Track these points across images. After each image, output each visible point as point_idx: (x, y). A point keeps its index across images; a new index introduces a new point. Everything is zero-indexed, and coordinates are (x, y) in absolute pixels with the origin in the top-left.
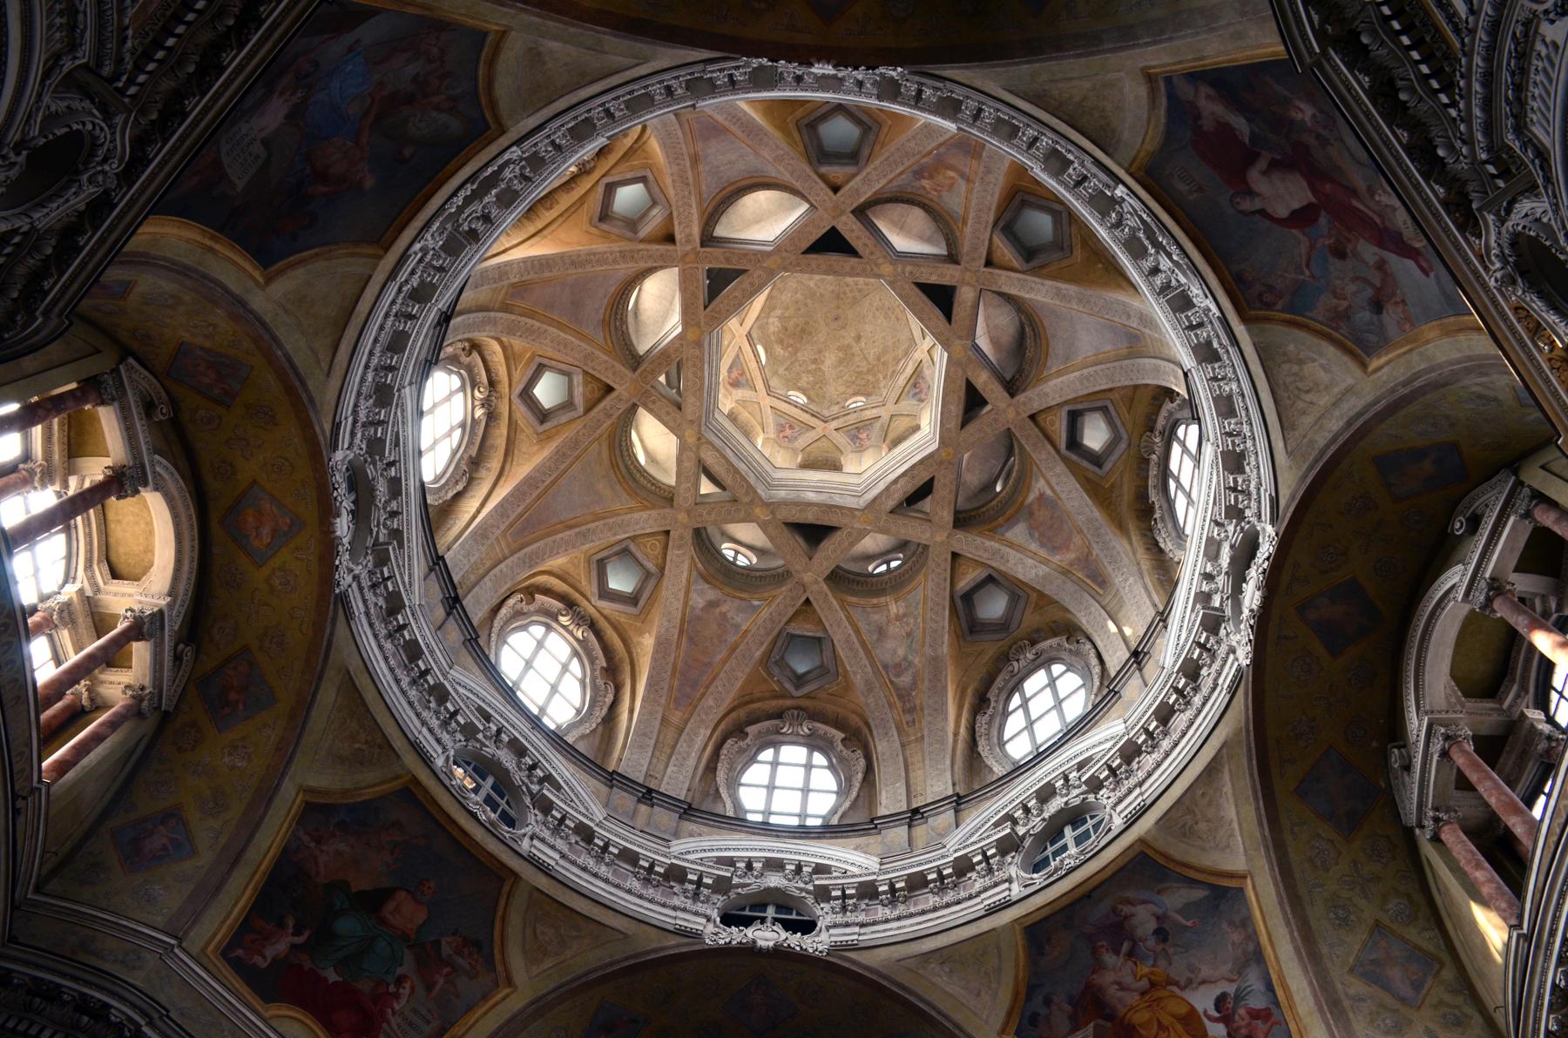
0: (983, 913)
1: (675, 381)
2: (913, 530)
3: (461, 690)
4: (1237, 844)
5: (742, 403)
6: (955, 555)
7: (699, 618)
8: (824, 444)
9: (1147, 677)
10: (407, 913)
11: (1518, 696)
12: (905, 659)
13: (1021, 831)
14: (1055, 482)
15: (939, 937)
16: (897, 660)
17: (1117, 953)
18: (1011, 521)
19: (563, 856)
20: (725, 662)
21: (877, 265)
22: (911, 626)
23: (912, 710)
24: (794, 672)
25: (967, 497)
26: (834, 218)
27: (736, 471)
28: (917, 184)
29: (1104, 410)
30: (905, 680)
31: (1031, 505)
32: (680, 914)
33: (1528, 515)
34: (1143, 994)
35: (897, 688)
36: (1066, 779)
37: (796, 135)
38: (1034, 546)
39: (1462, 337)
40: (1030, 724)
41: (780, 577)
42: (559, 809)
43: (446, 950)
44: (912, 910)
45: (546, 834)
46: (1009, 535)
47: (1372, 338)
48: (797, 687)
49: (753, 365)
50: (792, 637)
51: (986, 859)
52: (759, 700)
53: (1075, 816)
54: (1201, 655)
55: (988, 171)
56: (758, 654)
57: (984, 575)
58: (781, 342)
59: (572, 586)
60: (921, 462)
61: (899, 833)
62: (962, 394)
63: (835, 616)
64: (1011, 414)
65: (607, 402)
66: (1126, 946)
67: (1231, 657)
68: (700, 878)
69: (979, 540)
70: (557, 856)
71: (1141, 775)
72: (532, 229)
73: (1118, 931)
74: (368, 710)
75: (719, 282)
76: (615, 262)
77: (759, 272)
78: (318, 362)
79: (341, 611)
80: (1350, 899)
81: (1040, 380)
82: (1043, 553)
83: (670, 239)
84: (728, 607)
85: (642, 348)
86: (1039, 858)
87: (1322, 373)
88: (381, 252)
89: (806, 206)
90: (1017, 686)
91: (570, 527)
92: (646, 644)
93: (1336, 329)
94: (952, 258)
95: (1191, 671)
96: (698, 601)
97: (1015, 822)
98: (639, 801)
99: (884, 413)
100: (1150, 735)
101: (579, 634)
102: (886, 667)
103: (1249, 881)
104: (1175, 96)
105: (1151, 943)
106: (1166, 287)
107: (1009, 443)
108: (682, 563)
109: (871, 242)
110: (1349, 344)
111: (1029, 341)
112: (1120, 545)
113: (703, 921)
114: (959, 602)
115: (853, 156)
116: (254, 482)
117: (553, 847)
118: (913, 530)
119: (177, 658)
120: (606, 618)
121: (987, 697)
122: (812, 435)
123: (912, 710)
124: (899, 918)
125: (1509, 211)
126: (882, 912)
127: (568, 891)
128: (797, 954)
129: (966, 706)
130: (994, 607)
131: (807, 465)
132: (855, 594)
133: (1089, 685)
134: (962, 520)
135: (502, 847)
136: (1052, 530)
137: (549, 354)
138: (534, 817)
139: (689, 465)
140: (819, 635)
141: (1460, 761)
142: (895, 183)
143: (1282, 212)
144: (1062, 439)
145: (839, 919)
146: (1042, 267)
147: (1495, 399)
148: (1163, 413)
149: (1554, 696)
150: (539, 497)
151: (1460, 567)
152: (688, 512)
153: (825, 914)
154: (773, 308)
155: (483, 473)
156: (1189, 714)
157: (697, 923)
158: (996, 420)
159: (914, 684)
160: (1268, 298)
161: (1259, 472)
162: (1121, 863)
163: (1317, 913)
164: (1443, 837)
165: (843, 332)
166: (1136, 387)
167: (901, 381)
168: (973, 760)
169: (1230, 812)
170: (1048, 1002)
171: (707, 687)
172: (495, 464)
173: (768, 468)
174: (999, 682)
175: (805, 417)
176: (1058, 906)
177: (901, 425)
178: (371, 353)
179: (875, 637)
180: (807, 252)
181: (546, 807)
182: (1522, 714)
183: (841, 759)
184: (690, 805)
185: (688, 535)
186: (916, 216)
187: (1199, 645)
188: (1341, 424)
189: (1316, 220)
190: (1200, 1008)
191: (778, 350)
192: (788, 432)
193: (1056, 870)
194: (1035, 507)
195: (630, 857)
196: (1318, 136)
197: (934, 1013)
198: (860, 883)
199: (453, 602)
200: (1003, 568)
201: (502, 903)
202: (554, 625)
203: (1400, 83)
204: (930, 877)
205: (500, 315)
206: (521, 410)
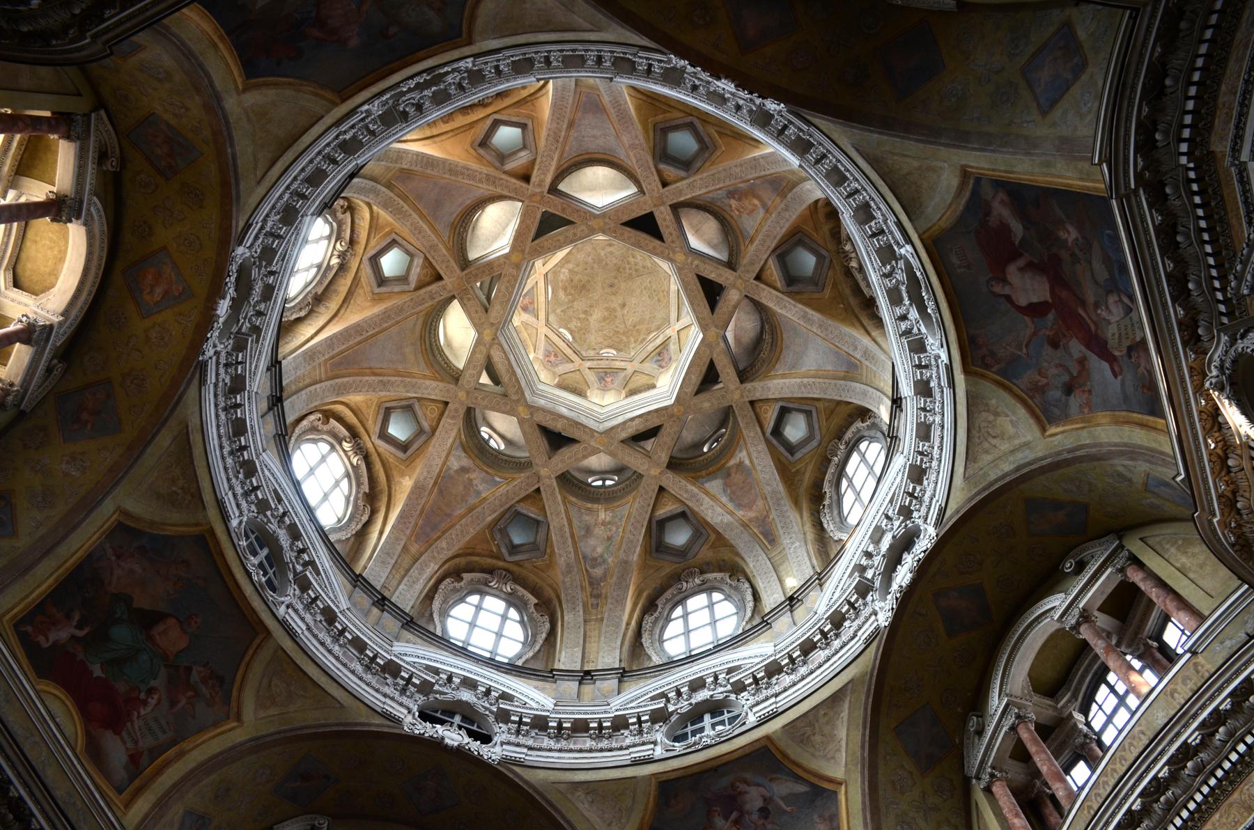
0: (628, 762)
1: (490, 288)
2: (634, 460)
3: (267, 472)
4: (841, 759)
5: (525, 325)
6: (661, 489)
7: (451, 477)
8: (577, 376)
9: (796, 618)
10: (171, 637)
11: (1069, 701)
12: (601, 556)
13: (671, 708)
14: (754, 456)
17: (726, 818)
18: (711, 476)
19: (309, 629)
20: (462, 517)
22: (613, 532)
23: (598, 596)
24: (511, 541)
25: (688, 446)
27: (514, 373)
28: (726, 201)
29: (808, 414)
30: (598, 572)
31: (729, 468)
32: (388, 701)
33: (1122, 570)
35: (590, 577)
36: (716, 678)
38: (724, 499)
39: (1126, 428)
40: (687, 632)
41: (522, 466)
42: (315, 591)
44: (572, 746)
45: (300, 607)
46: (707, 485)
47: (1057, 412)
48: (510, 554)
49: (542, 299)
50: (518, 514)
51: (640, 722)
52: (478, 555)
53: (715, 708)
54: (848, 611)
55: (787, 209)
56: (490, 519)
57: (680, 510)
58: (565, 289)
59: (361, 422)
60: (657, 411)
61: (572, 686)
62: (704, 369)
63: (556, 506)
64: (736, 396)
65: (434, 287)
66: (734, 815)
67: (873, 617)
68: (411, 677)
69: (684, 482)
70: (304, 628)
71: (777, 689)
72: (428, 133)
73: (732, 803)
74: (192, 463)
75: (550, 224)
76: (480, 181)
77: (583, 227)
78: (255, 169)
79: (197, 375)
81: (766, 376)
82: (730, 506)
83: (526, 178)
84: (476, 476)
85: (473, 255)
86: (680, 732)
87: (1010, 427)
88: (338, 100)
89: (633, 190)
90: (682, 602)
91: (375, 374)
92: (405, 485)
93: (1031, 398)
94: (731, 265)
95: (837, 620)
96: (455, 464)
97: (668, 700)
98: (373, 604)
99: (630, 368)
100: (792, 661)
101: (355, 461)
102: (584, 557)
104: (977, 191)
105: (755, 817)
106: (907, 332)
107: (726, 416)
108: (450, 430)
110: (1038, 411)
111: (766, 347)
112: (793, 515)
113: (406, 712)
115: (686, 164)
116: (165, 248)
117: (303, 619)
118: (634, 460)
119: (49, 370)
120: (379, 455)
121: (658, 600)
122: (570, 367)
123: (598, 596)
124: (560, 751)
125: (1243, 337)
126: (547, 742)
127: (305, 657)
129: (640, 605)
130: (679, 537)
131: (561, 386)
132: (576, 496)
133: (741, 614)
134: (674, 465)
135: (264, 607)
136: (742, 491)
137: (403, 234)
138: (293, 590)
139: (480, 358)
140: (540, 518)
141: (1024, 735)
143: (1023, 302)
145: (513, 738)
146: (798, 293)
147: (1130, 480)
148: (853, 429)
149: (1094, 707)
150: (359, 343)
151: (1063, 595)
152: (468, 393)
153: (501, 733)
154: (568, 262)
155: (322, 309)
156: (827, 652)
157: (400, 712)
158: (723, 397)
159: (605, 575)
161: (936, 488)
162: (747, 751)
164: (994, 789)
165: (613, 298)
166: (839, 403)
167: (650, 347)
168: (636, 647)
169: (842, 733)
171: (444, 532)
172: (333, 305)
173: (535, 379)
174: (668, 594)
175: (569, 352)
176: (690, 772)
177: (640, 380)
178: (295, 179)
179: (583, 533)
181: (305, 585)
182: (1071, 714)
183: (531, 619)
184: (412, 620)
185: (462, 411)
186: (711, 226)
187: (849, 603)
188: (1012, 467)
189: (1046, 315)
191: (561, 294)
192: (552, 359)
193: (695, 744)
194: (734, 470)
195: (359, 645)
196: (1073, 255)
198: (536, 716)
199: (276, 400)
200: (696, 509)
201: (251, 652)
202: (338, 447)
203: (1180, 229)
205: (384, 189)
206: (367, 270)
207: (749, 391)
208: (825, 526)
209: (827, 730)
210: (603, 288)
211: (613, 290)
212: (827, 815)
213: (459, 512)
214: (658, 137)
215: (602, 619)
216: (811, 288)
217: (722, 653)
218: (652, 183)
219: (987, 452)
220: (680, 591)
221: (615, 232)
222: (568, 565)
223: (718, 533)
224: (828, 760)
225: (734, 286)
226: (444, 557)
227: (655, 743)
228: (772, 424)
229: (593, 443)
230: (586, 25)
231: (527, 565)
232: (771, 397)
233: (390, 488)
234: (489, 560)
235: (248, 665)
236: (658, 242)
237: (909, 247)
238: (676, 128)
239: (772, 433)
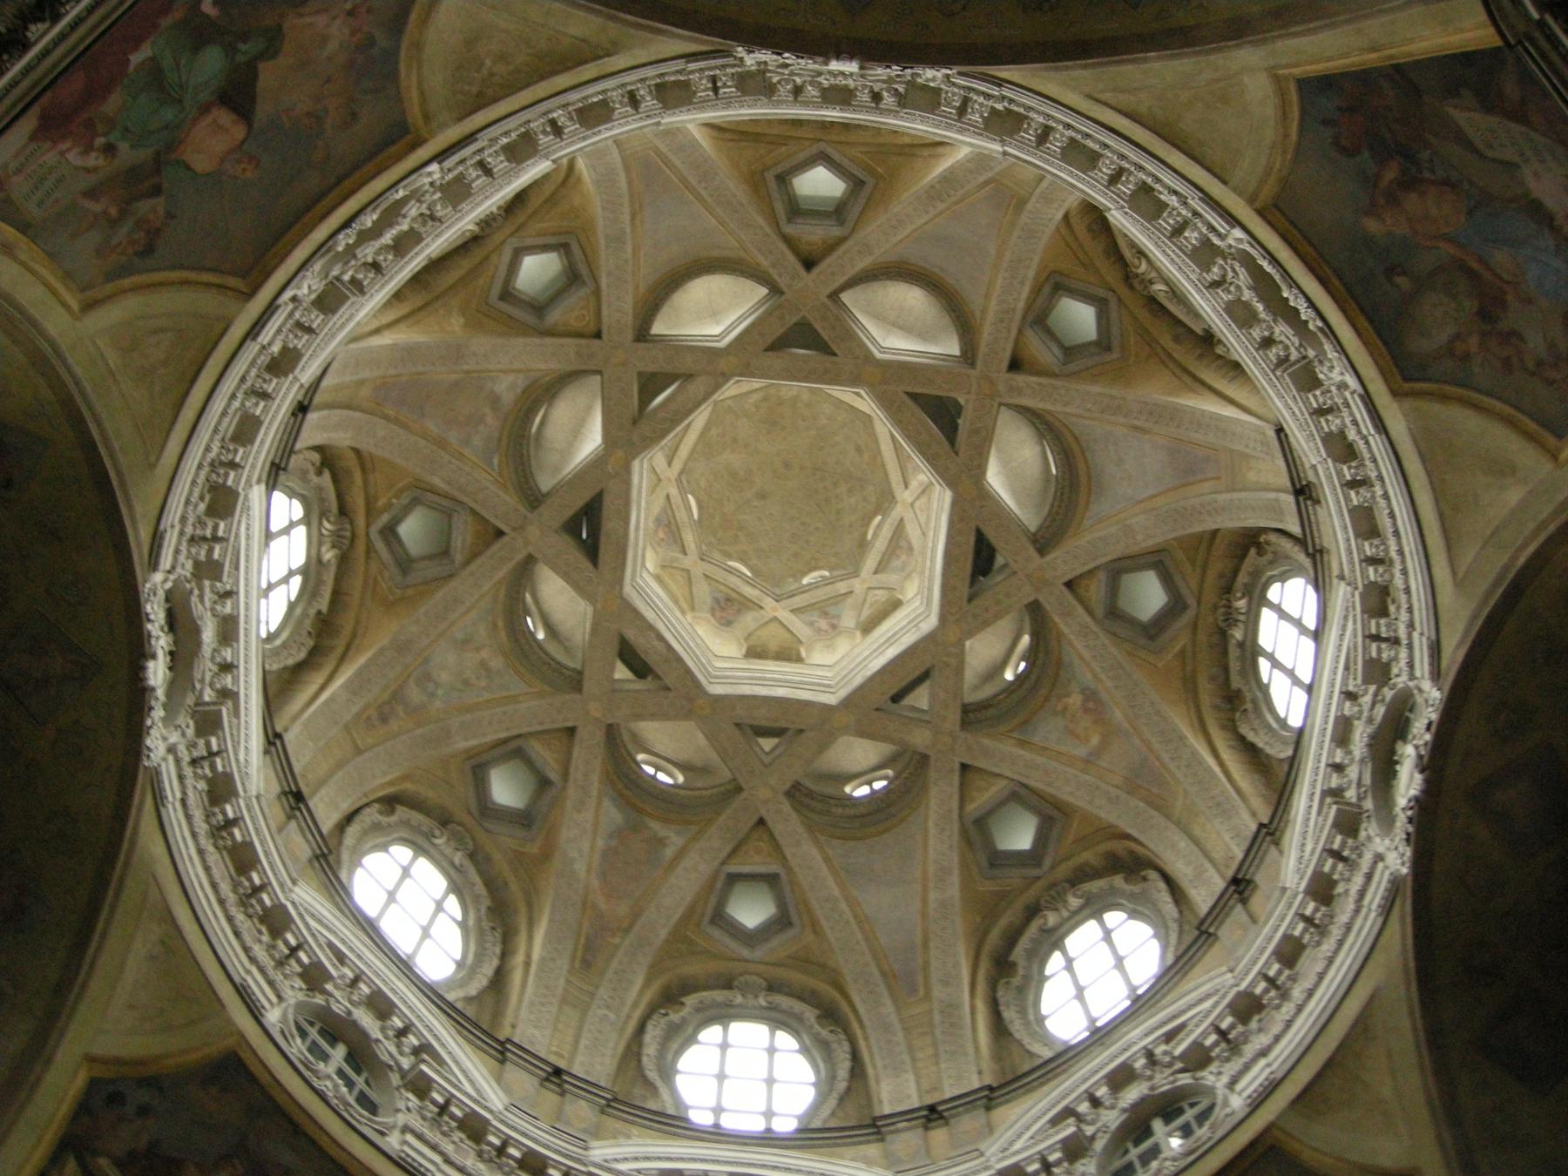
6: (571, 731)
12: (437, 685)
15: (196, 927)
26: (1028, 576)
30: (415, 695)
35: (401, 687)
38: (600, 843)
43: (143, 207)
46: (606, 803)
48: (381, 532)
50: (450, 517)
51: (294, 951)
52: (366, 482)
53: (361, 1056)
56: (437, 481)
58: (765, 399)
59: (535, 213)
60: (688, 671)
64: (764, 793)
71: (449, 1148)
82: (597, 858)
83: (1015, 365)
88: (1258, 204)
90: (419, 850)
102: (426, 661)
114: (513, 745)
120: (487, 258)
124: (201, 852)
128: (141, 722)
130: (505, 790)
140: (458, 558)
142: (1076, 662)
150: (683, 180)
157: (166, 561)
167: (733, 581)
170: (143, 1111)
171: (396, 421)
174: (417, 817)
193: (315, 1072)
197: (91, 951)
200: (569, 804)
204: (255, 876)
208: (648, 1038)
213: (432, 426)
215: (359, 752)
216: (984, 862)
217: (443, 1017)
218: (1065, 561)
220: (429, 836)
223: (547, 855)
226: (366, 445)
227: (280, 997)
228: (746, 869)
230: (1464, 563)
231: (374, 566)
232: (789, 856)
233: (437, 298)
235: (185, 283)
237: (1237, 1102)
238: (1167, 580)
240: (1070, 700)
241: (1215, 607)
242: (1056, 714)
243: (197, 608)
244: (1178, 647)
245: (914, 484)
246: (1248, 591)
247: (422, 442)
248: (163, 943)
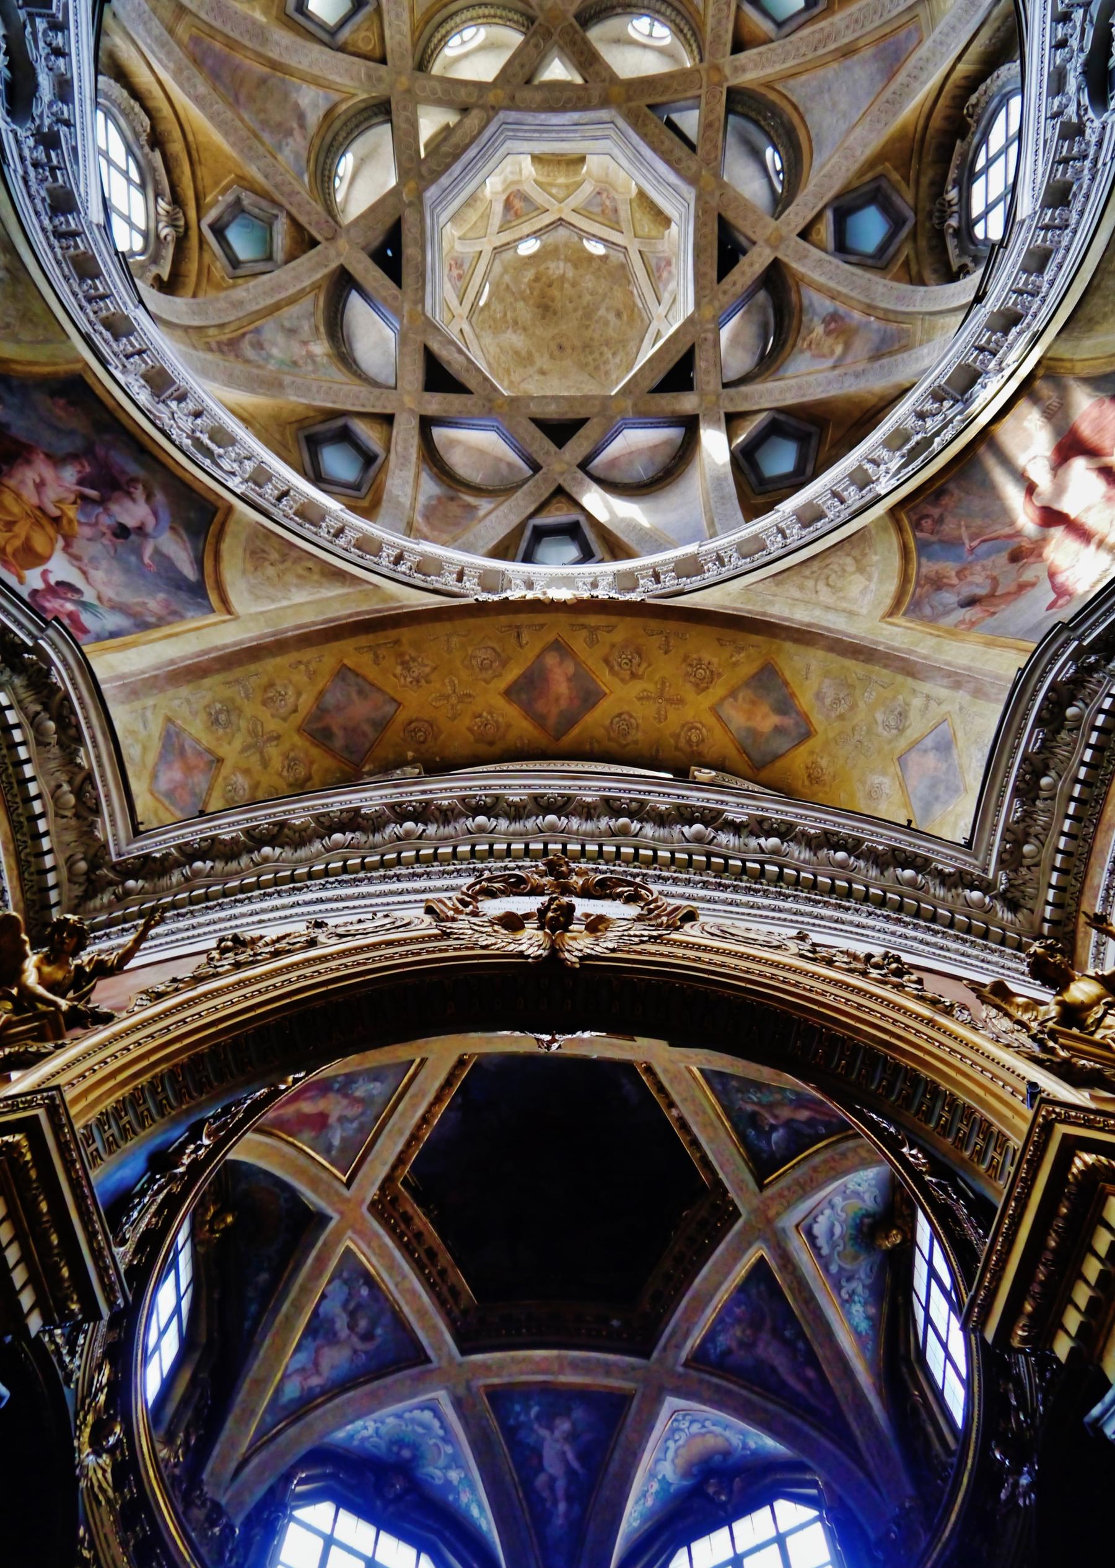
12: (270, 356)
16: (266, 345)
17: (81, 482)
21: (711, 301)
24: (227, 226)
27: (456, 157)
28: (817, 321)
34: (40, 508)
37: (869, 176)
48: (212, 227)
50: (271, 226)
56: (253, 171)
58: (537, 279)
62: (571, 416)
63: (310, 271)
64: (557, 467)
66: (93, 493)
73: (106, 485)
80: (239, 729)
83: (738, 46)
93: (918, 584)
102: (257, 331)
103: (228, 617)
105: (105, 520)
109: (739, 289)
114: (339, 422)
115: (842, 247)
122: (454, 302)
144: (541, 520)
152: (409, 91)
160: (927, 524)
162: (196, 486)
163: (213, 688)
165: (546, 356)
169: (299, 597)
180: (721, 218)
190: (49, 566)
191: (530, 274)
207: (574, 479)
209: (290, 578)
210: (553, 338)
211: (557, 353)
212: (175, 606)
214: (866, 189)
218: (798, 214)
219: (801, 588)
221: (705, 212)
222: (241, 303)
224: (251, 592)
225: (703, 395)
229: (406, 307)
231: (207, 257)
234: (190, 194)
236: (714, 274)
238: (888, 210)
239: (535, 528)
240: (814, 335)
241: (930, 215)
242: (802, 351)
243: (33, 54)
244: (902, 259)
245: (666, 297)
246: (957, 183)
247: (239, 124)
248: (8, 270)
